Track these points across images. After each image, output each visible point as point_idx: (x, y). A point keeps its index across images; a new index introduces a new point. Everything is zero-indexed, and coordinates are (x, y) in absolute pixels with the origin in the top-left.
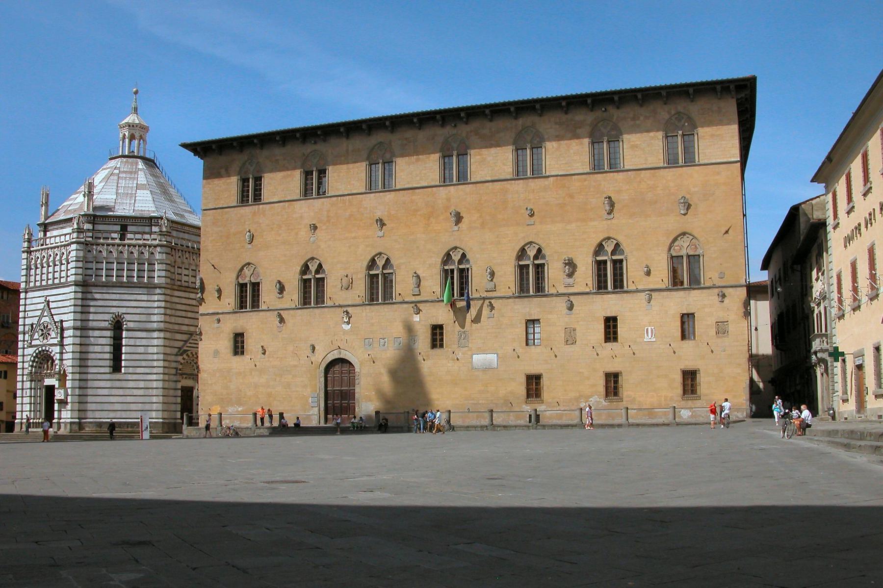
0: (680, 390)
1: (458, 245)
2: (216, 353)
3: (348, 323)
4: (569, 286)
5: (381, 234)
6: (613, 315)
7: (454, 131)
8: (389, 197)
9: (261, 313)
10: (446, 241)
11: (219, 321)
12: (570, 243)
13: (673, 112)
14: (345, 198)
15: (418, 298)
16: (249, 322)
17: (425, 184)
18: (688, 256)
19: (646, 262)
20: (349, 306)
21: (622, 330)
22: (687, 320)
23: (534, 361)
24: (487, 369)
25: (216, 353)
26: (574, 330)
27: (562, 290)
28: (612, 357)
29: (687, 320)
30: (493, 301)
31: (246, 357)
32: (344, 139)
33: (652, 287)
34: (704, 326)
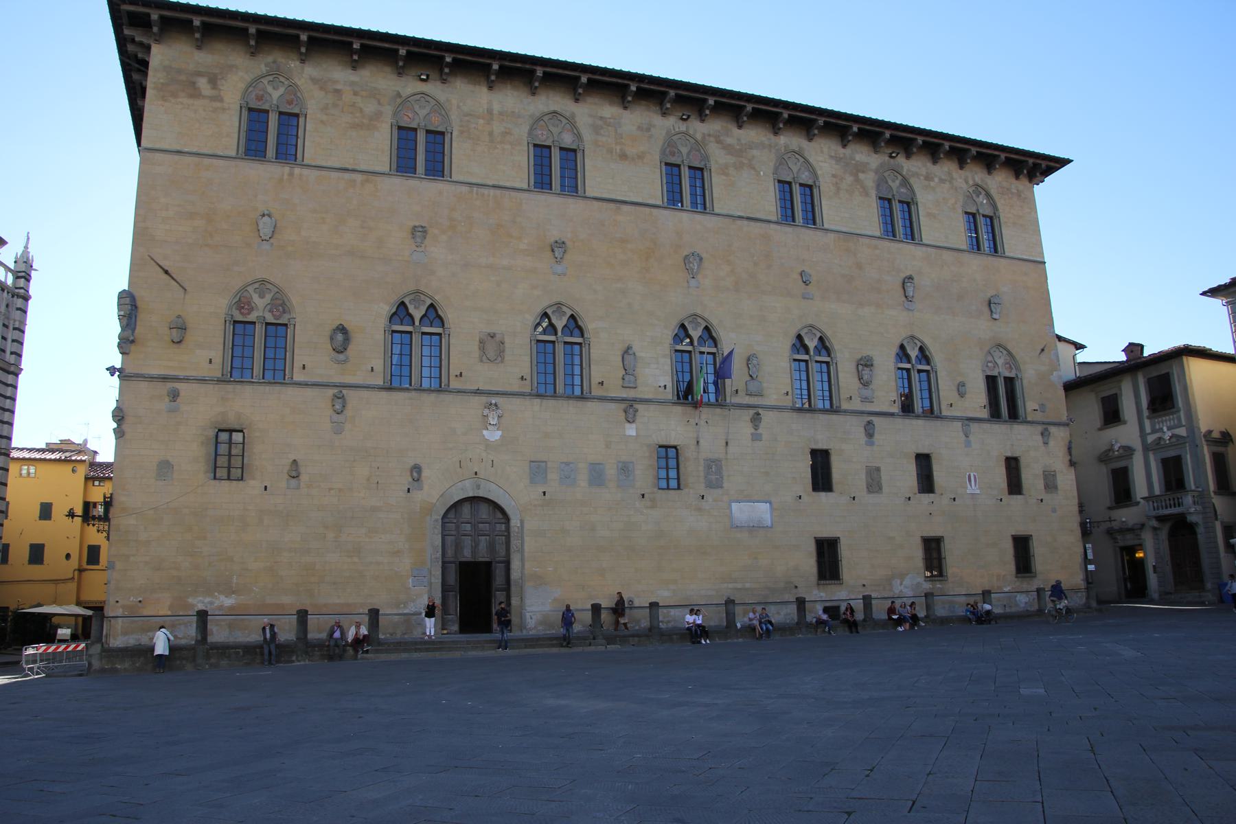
0: (1011, 567)
1: (699, 312)
2: (165, 468)
3: (498, 426)
4: (865, 400)
5: (559, 268)
6: (926, 451)
7: (682, 127)
8: (573, 206)
9: (290, 392)
10: (680, 301)
11: (174, 395)
12: (866, 333)
13: (971, 183)
14: (485, 191)
15: (631, 394)
16: (254, 405)
17: (640, 200)
18: (1005, 378)
19: (961, 382)
20: (497, 394)
21: (940, 475)
22: (1013, 465)
23: (826, 515)
24: (754, 528)
25: (165, 468)
26: (878, 469)
27: (856, 405)
28: (929, 516)
29: (1013, 465)
30: (760, 411)
31: (252, 487)
32: (485, 89)
33: (971, 415)
34: (1031, 477)
